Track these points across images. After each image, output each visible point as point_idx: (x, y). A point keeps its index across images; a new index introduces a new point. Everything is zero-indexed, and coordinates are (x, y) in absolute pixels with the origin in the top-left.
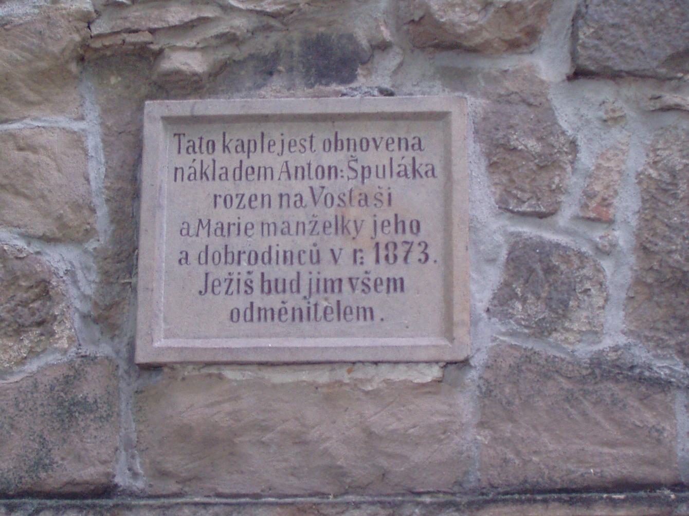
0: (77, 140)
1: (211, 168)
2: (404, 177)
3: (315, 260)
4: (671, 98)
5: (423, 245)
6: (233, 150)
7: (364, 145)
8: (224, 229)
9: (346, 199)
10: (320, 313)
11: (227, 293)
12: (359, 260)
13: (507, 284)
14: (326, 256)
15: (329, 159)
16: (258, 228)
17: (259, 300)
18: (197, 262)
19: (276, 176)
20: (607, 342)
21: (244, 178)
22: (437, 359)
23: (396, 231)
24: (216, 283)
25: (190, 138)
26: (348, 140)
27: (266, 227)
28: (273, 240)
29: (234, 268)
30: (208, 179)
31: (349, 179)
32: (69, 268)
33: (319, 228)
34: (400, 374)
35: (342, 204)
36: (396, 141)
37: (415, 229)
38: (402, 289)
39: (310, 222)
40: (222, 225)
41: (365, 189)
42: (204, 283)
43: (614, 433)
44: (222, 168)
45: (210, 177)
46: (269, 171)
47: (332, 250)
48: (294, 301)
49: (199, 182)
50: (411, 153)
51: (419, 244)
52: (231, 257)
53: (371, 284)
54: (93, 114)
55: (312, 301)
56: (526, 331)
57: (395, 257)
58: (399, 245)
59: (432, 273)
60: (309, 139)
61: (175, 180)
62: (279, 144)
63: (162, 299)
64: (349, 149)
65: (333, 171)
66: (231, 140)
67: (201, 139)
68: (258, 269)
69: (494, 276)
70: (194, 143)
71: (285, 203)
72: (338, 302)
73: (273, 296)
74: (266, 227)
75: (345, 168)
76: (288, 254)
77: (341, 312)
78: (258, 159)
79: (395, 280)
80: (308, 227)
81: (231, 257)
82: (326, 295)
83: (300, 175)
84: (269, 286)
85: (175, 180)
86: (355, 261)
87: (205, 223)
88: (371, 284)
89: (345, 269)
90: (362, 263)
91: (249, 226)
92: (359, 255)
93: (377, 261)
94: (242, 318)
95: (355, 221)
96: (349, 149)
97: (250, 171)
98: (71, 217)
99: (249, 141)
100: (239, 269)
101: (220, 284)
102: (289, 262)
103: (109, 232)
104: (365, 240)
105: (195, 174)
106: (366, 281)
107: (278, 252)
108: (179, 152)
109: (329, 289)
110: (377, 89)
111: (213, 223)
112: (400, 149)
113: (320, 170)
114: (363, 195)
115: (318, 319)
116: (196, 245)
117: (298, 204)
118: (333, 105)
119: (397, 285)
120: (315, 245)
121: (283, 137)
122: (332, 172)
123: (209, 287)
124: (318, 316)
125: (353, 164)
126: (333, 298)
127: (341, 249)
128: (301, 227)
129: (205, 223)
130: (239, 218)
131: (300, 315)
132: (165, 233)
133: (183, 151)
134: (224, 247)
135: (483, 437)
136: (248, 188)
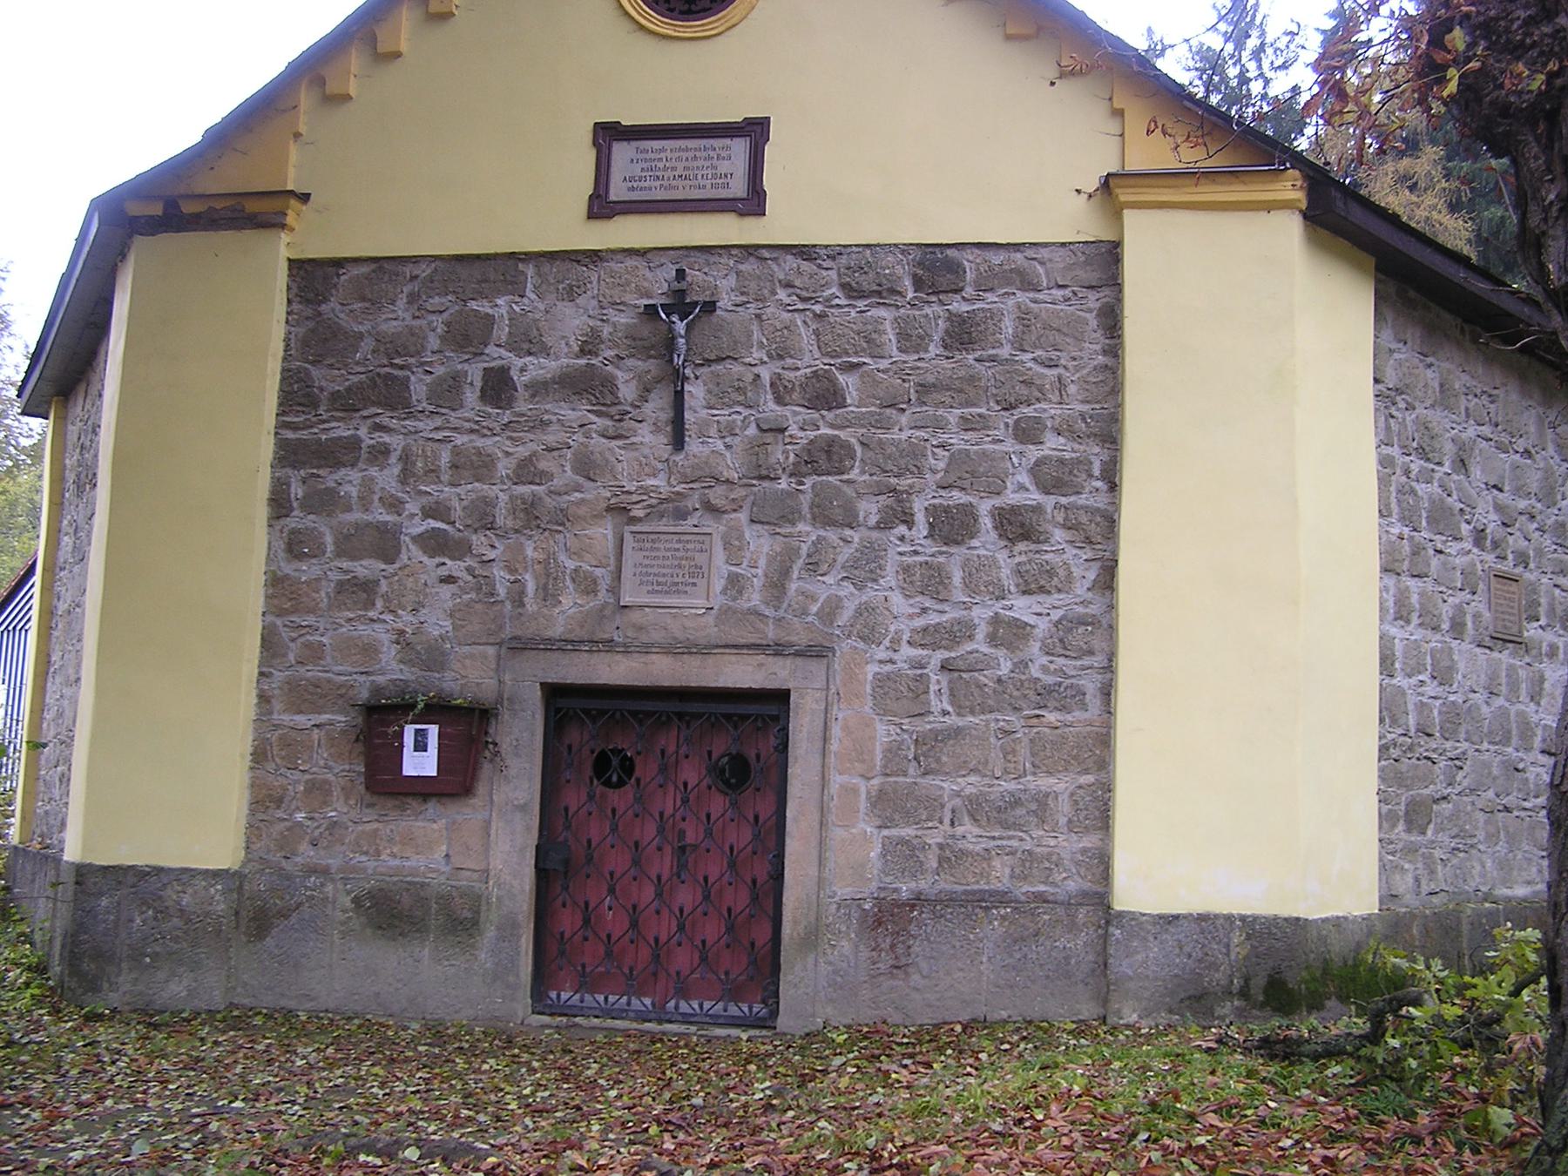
0: (605, 536)
4: (778, 530)
7: (688, 542)
8: (646, 566)
15: (677, 546)
34: (693, 611)
54: (610, 527)
59: (705, 580)
69: (723, 582)
77: (678, 592)
84: (659, 584)
89: (680, 579)
104: (686, 571)
118: (678, 529)
119: (694, 584)
131: (667, 592)
135: (716, 629)
136: (654, 554)
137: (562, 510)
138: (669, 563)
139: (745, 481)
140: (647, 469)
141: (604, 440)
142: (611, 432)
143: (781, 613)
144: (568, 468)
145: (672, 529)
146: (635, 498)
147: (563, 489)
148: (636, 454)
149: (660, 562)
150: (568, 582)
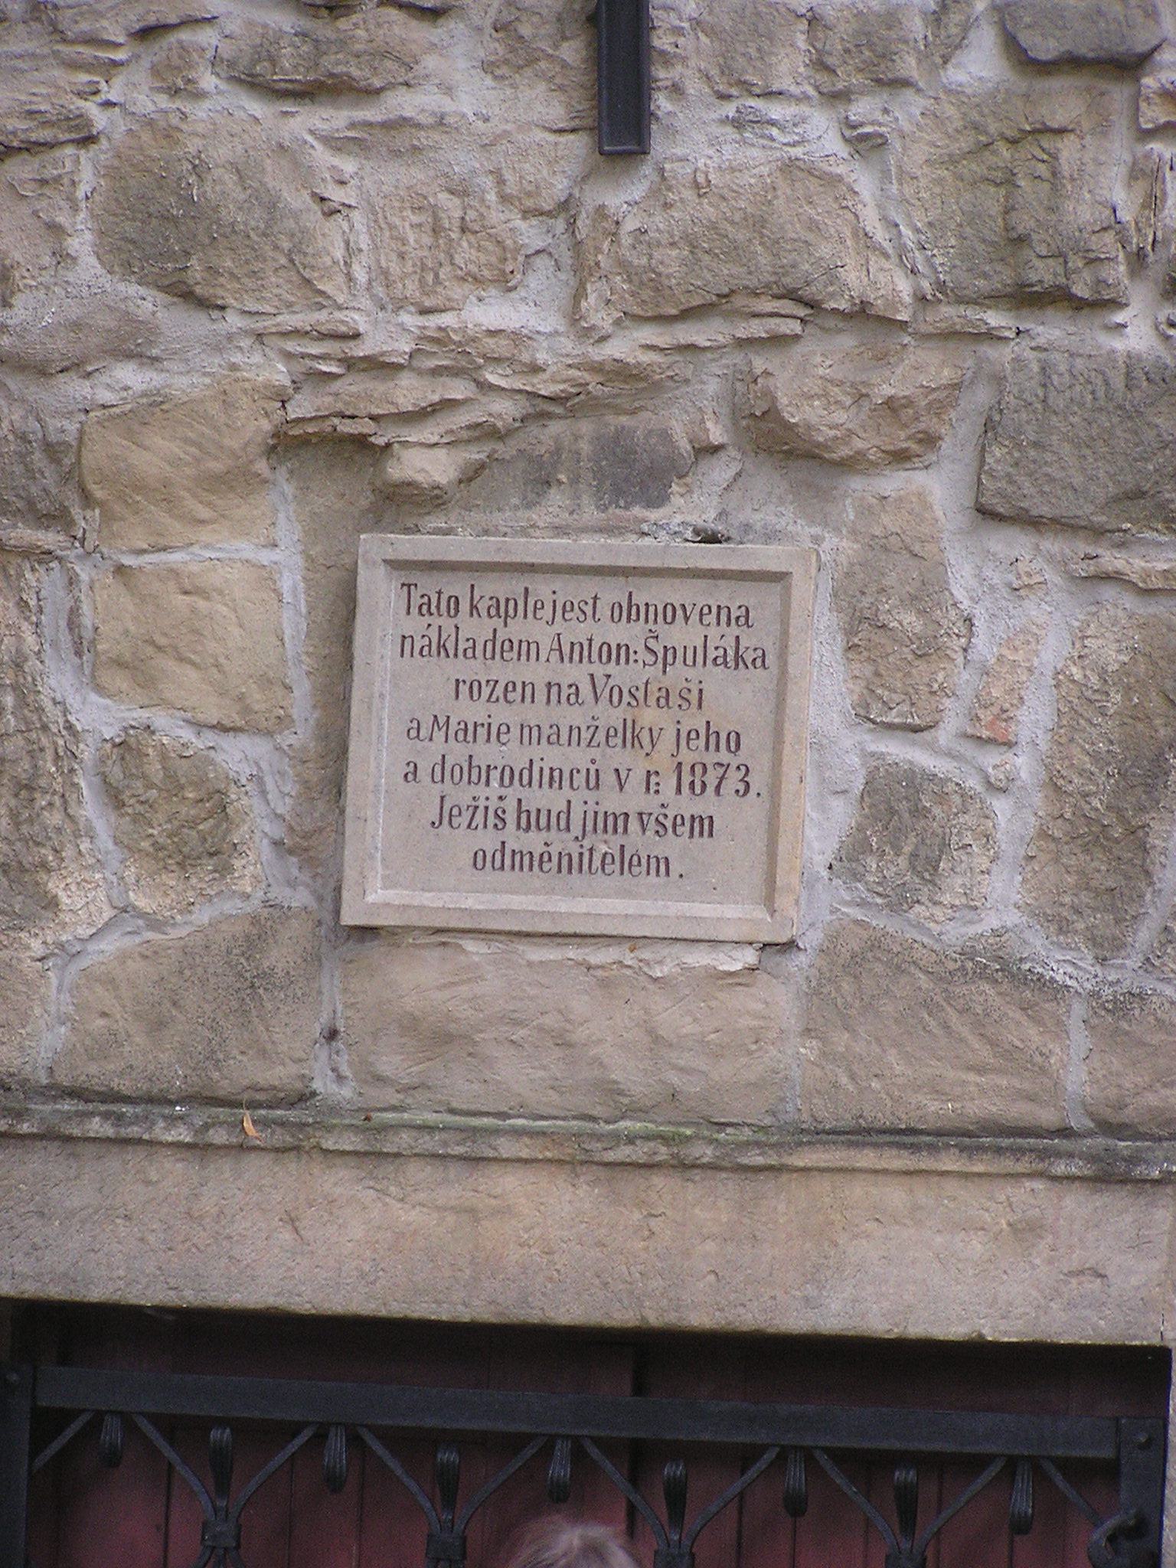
0: (267, 577)
1: (453, 638)
2: (722, 667)
3: (592, 783)
4: (1112, 560)
5: (743, 768)
6: (484, 613)
7: (671, 613)
8: (468, 732)
9: (640, 695)
10: (597, 863)
11: (469, 826)
12: (653, 788)
13: (860, 828)
14: (609, 779)
15: (618, 634)
16: (515, 732)
17: (516, 840)
18: (430, 779)
19: (543, 657)
20: (992, 921)
21: (498, 656)
22: (750, 939)
23: (707, 748)
24: (455, 811)
25: (425, 592)
26: (647, 604)
27: (526, 731)
28: (536, 752)
29: (481, 791)
30: (448, 656)
31: (645, 664)
32: (255, 773)
33: (600, 736)
34: (699, 958)
35: (634, 703)
36: (714, 610)
37: (733, 745)
38: (711, 835)
39: (588, 727)
40: (466, 725)
41: (666, 682)
42: (438, 811)
43: (984, 1053)
44: (468, 640)
45: (451, 653)
46: (533, 647)
47: (617, 770)
48: (561, 842)
49: (434, 659)
50: (734, 630)
51: (738, 768)
52: (475, 772)
53: (669, 824)
54: (288, 531)
55: (587, 843)
56: (879, 900)
57: (704, 785)
58: (710, 768)
59: (753, 810)
60: (591, 602)
61: (402, 656)
62: (549, 607)
63: (380, 832)
64: (647, 621)
65: (623, 650)
66: (482, 597)
67: (439, 593)
68: (513, 793)
69: (842, 814)
70: (429, 599)
71: (554, 697)
72: (622, 846)
73: (533, 834)
74: (526, 731)
75: (641, 649)
76: (556, 774)
77: (626, 862)
78: (518, 629)
79: (702, 819)
80: (586, 735)
81: (475, 772)
82: (606, 836)
83: (576, 657)
84: (528, 820)
85: (402, 656)
86: (648, 789)
87: (442, 720)
88: (669, 824)
89: (634, 800)
90: (657, 792)
91: (504, 729)
92: (654, 779)
93: (679, 791)
94: (489, 864)
95: (651, 730)
96: (647, 621)
97: (507, 644)
98: (258, 696)
99: (507, 600)
100: (487, 792)
101: (460, 814)
102: (556, 785)
103: (312, 722)
104: (662, 759)
105: (430, 645)
106: (661, 818)
107: (542, 769)
108: (408, 613)
109: (610, 828)
110: (691, 529)
111: (453, 721)
112: (718, 624)
113: (605, 648)
114: (664, 690)
115: (593, 871)
116: (428, 755)
117: (573, 699)
118: (625, 550)
119: (703, 826)
120: (593, 762)
121: (554, 597)
122: (621, 653)
123: (446, 817)
124: (594, 867)
125: (652, 643)
126: (617, 840)
127: (629, 770)
128: (575, 732)
129: (442, 720)
130: (489, 716)
131: (568, 865)
132: (385, 735)
133: (414, 610)
134: (467, 758)
135: (809, 1050)
136: (503, 672)
137: (53, 450)
138: (571, 716)
139: (949, 313)
140: (466, 253)
141: (256, 107)
142: (290, 66)
143: (1126, 972)
144: (81, 243)
145: (591, 549)
146: (408, 392)
147: (61, 346)
148: (414, 175)
149: (537, 713)
150: (91, 809)
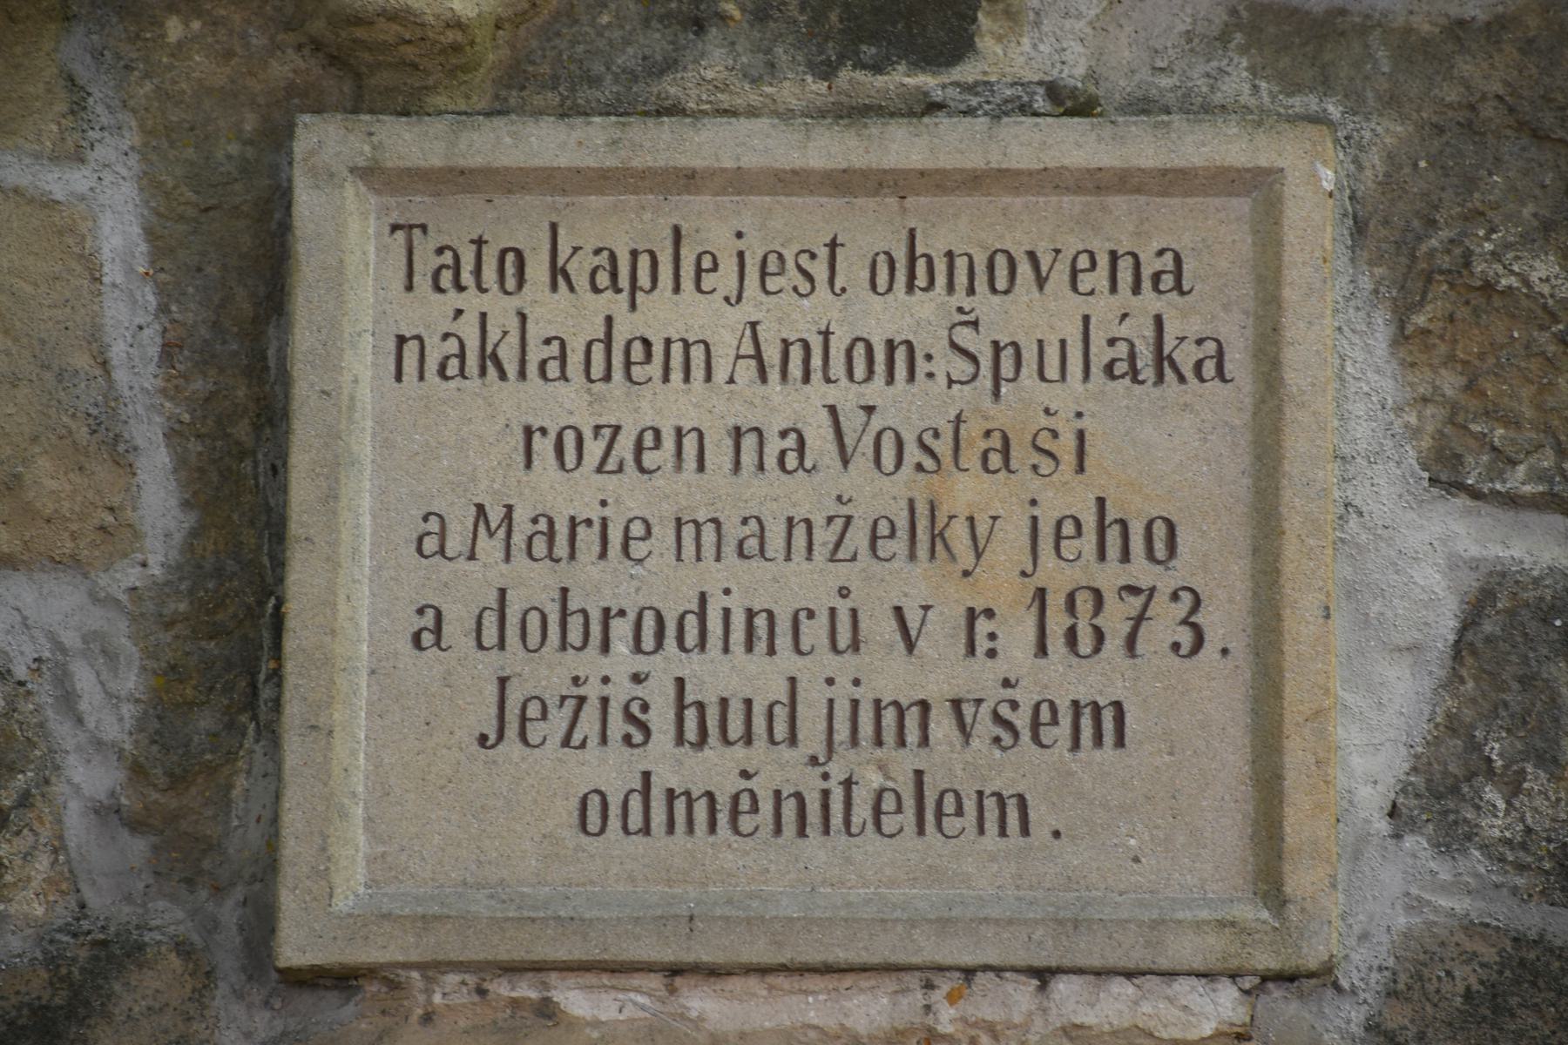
1: (514, 339)
2: (1127, 381)
3: (844, 640)
5: (1186, 597)
6: (581, 282)
9: (943, 447)
10: (862, 812)
11: (566, 742)
12: (982, 645)
13: (1452, 725)
14: (877, 627)
16: (664, 534)
18: (473, 643)
19: (721, 374)
21: (618, 374)
22: (1234, 963)
23: (1102, 555)
24: (533, 710)
25: (446, 241)
26: (950, 255)
27: (688, 532)
28: (713, 576)
29: (589, 663)
30: (503, 376)
31: (951, 382)
32: (47, 654)
33: (858, 538)
35: (929, 463)
36: (1103, 261)
37: (1160, 550)
38: (1120, 742)
39: (830, 519)
40: (551, 522)
41: (1001, 416)
42: (494, 710)
44: (548, 341)
45: (511, 369)
46: (697, 353)
47: (898, 610)
49: (474, 384)
50: (1150, 302)
51: (1175, 597)
53: (1022, 720)
55: (837, 771)
57: (1099, 636)
58: (1110, 598)
60: (823, 253)
61: (399, 377)
62: (729, 266)
63: (362, 761)
64: (951, 287)
65: (901, 355)
66: (576, 249)
67: (479, 243)
68: (665, 666)
70: (457, 258)
71: (749, 458)
72: (919, 774)
73: (713, 752)
74: (688, 532)
75: (940, 348)
76: (761, 622)
79: (1097, 709)
82: (879, 753)
83: (795, 369)
85: (399, 377)
86: (971, 649)
87: (495, 515)
88: (1022, 720)
90: (992, 653)
91: (637, 529)
92: (983, 626)
93: (1042, 650)
94: (614, 822)
95: (971, 519)
96: (951, 287)
97: (637, 351)
99: (634, 254)
100: (605, 665)
101: (544, 716)
102: (761, 646)
103: (178, 537)
105: (462, 356)
106: (1005, 711)
107: (727, 612)
108: (409, 287)
109: (889, 736)
110: (1041, 91)
111: (521, 516)
112: (1114, 288)
113: (860, 350)
114: (997, 434)
115: (854, 830)
117: (791, 460)
120: (844, 592)
121: (741, 244)
124: (856, 820)
125: (964, 337)
126: (904, 763)
127: (926, 608)
128: (800, 532)
129: (495, 515)
130: (604, 503)
132: (366, 548)
133: (422, 281)
134: (557, 596)
